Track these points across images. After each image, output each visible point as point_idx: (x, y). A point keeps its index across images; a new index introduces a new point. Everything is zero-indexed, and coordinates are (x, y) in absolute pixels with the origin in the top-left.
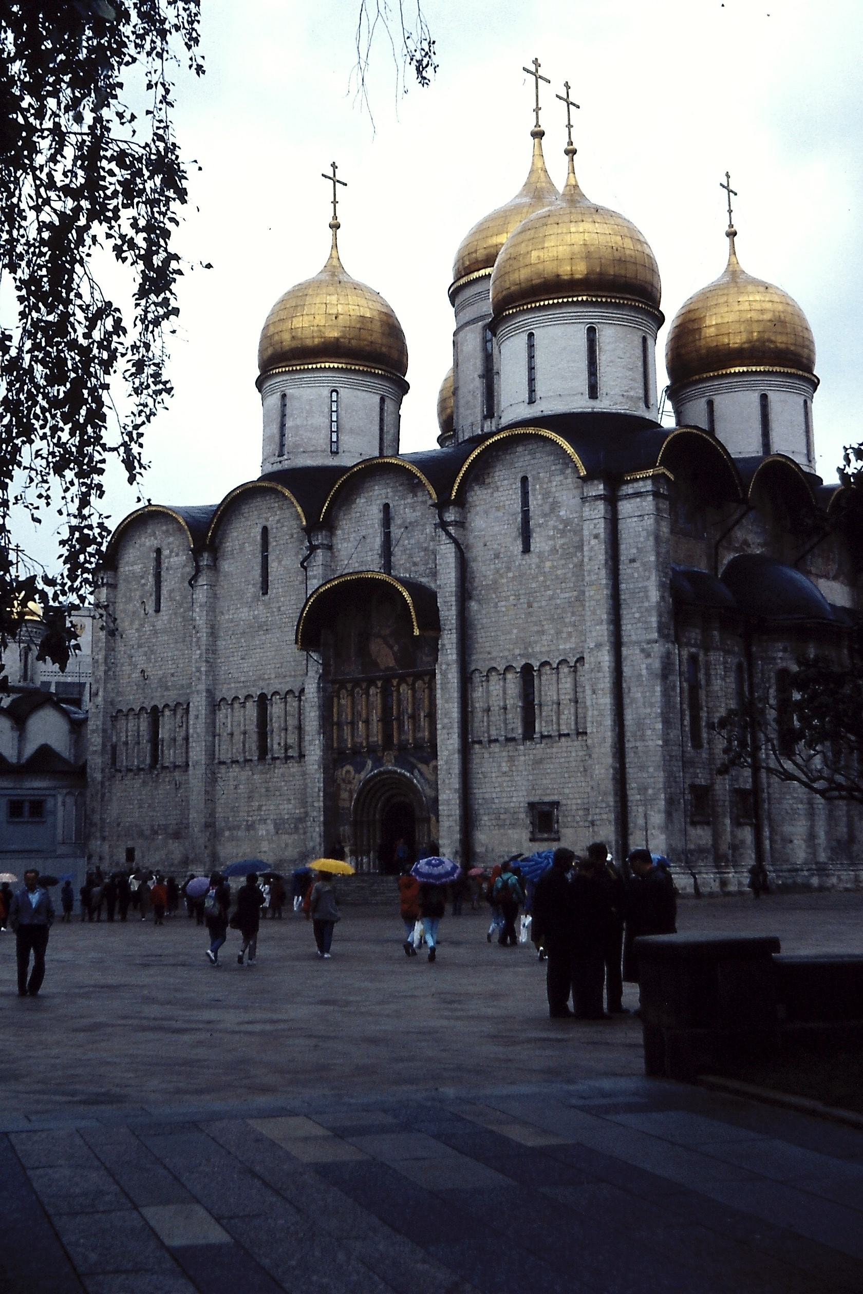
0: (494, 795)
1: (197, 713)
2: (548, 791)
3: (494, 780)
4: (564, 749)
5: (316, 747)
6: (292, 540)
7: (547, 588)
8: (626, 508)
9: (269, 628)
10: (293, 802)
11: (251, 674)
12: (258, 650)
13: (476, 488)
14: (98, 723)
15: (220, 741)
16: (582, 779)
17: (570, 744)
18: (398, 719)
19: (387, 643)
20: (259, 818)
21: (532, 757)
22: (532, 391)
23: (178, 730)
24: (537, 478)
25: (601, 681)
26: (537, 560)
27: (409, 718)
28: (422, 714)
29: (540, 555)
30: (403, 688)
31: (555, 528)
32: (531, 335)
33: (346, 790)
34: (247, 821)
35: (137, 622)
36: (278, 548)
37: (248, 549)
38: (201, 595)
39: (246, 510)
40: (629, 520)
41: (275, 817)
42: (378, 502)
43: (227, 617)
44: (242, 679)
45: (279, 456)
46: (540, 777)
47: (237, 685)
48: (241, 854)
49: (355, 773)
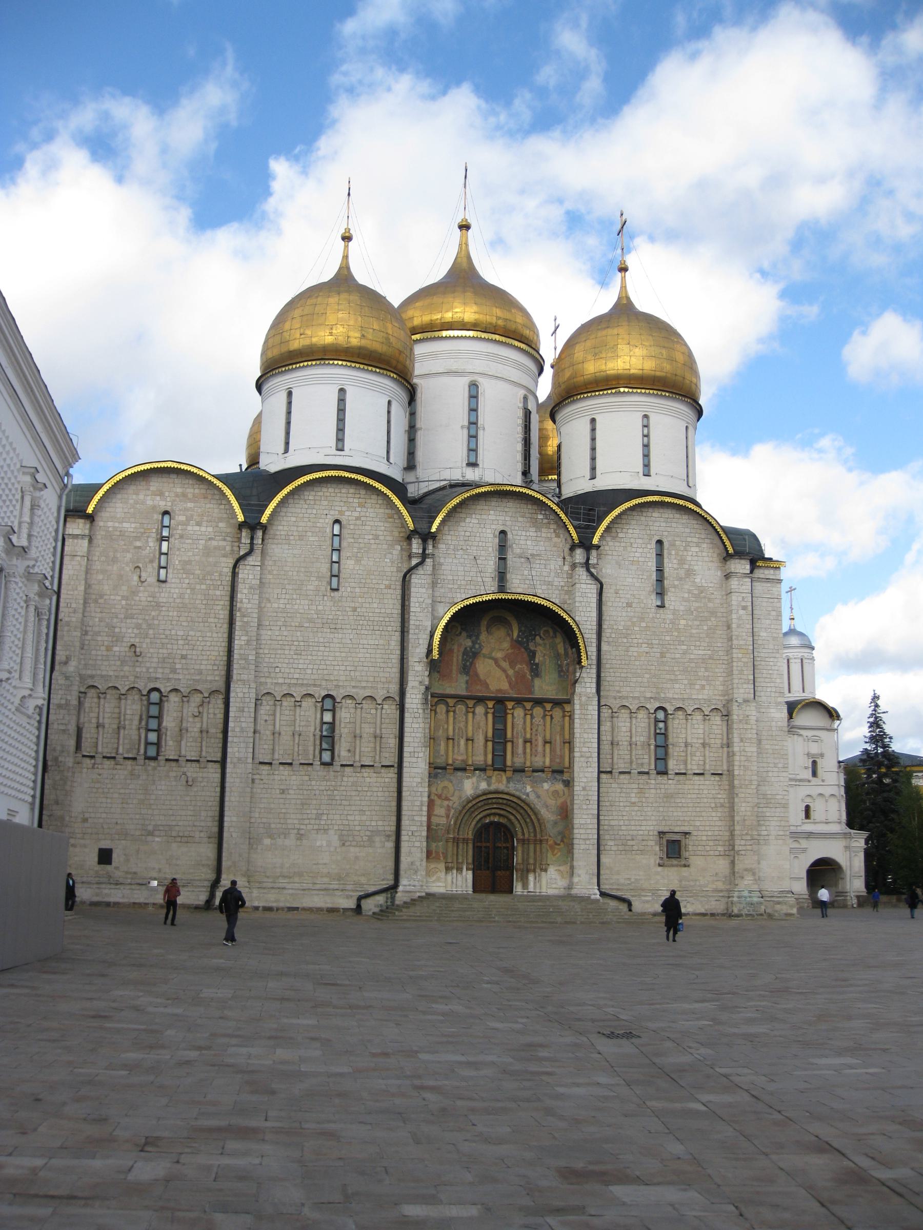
0: (621, 823)
1: (241, 705)
2: (679, 823)
3: (621, 808)
4: (696, 787)
5: (419, 760)
6: (377, 541)
7: (682, 643)
9: (339, 626)
10: (367, 813)
11: (309, 671)
12: (322, 649)
13: (608, 539)
14: (69, 697)
15: (259, 739)
16: (714, 814)
17: (702, 782)
18: (512, 742)
19: (499, 666)
20: (316, 827)
21: (663, 791)
22: (647, 466)
23: (191, 719)
24: (673, 544)
25: (749, 731)
26: (671, 617)
27: (525, 742)
29: (675, 612)
30: (519, 712)
31: (689, 592)
32: (646, 416)
34: (299, 829)
35: (124, 588)
36: (356, 545)
37: (311, 539)
38: (248, 574)
40: (760, 599)
41: (341, 827)
42: (493, 527)
43: (276, 605)
44: (296, 676)
45: (338, 450)
46: (671, 809)
47: (287, 681)
48: (287, 865)
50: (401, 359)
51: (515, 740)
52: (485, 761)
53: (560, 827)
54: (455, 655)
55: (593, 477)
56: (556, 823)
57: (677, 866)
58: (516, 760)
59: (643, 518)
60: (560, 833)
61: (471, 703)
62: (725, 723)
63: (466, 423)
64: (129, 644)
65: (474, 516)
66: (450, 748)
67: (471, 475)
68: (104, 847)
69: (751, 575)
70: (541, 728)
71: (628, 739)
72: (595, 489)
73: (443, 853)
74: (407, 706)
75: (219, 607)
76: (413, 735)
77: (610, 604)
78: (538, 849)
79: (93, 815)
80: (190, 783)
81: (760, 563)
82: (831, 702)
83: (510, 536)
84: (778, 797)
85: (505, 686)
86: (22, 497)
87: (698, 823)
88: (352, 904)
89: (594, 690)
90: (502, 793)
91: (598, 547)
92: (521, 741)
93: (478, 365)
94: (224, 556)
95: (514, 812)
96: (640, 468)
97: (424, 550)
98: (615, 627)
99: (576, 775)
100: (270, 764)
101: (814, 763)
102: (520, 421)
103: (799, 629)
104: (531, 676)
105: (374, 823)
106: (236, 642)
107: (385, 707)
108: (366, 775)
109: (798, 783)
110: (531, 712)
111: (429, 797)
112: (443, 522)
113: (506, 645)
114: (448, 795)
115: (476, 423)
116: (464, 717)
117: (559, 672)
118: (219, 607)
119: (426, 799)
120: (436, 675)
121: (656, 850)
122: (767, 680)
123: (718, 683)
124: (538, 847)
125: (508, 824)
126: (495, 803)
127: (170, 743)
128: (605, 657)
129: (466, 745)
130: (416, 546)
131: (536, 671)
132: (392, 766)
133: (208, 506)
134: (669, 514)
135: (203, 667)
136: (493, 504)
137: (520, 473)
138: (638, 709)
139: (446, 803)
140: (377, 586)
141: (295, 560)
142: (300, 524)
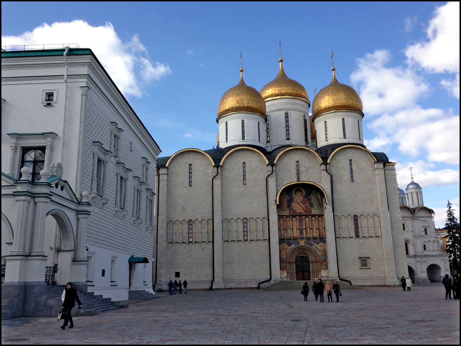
8: (387, 172)
14: (164, 225)
19: (299, 205)
20: (244, 261)
22: (345, 135)
27: (310, 230)
28: (315, 228)
30: (307, 219)
32: (343, 119)
33: (284, 252)
38: (217, 182)
39: (235, 156)
44: (234, 213)
45: (243, 139)
47: (232, 214)
49: (288, 246)
50: (261, 108)
51: (306, 229)
52: (297, 236)
53: (323, 257)
54: (285, 202)
55: (327, 141)
56: (322, 255)
57: (366, 269)
58: (307, 235)
59: (344, 153)
61: (291, 218)
62: (378, 219)
63: (285, 126)
64: (182, 206)
65: (288, 157)
66: (285, 232)
67: (288, 143)
68: (177, 272)
69: (384, 168)
70: (314, 224)
72: (328, 144)
74: (270, 220)
75: (209, 193)
76: (273, 229)
77: (335, 182)
78: (317, 265)
79: (173, 261)
80: (203, 249)
81: (387, 164)
82: (430, 208)
83: (300, 162)
84: (401, 244)
85: (302, 211)
86: (143, 167)
87: (372, 254)
88: (257, 286)
89: (332, 211)
90: (303, 246)
91: (329, 163)
92: (308, 229)
93: (288, 106)
94: (210, 176)
96: (343, 137)
97: (272, 169)
100: (228, 241)
101: (426, 230)
102: (303, 123)
103: (415, 182)
105: (262, 259)
106: (215, 203)
107: (263, 220)
108: (259, 243)
109: (420, 237)
110: (311, 219)
111: (279, 249)
112: (278, 160)
113: (301, 198)
114: (286, 248)
115: (288, 126)
118: (209, 193)
119: (278, 250)
120: (278, 209)
121: (358, 263)
122: (393, 204)
123: (375, 206)
124: (317, 264)
125: (307, 257)
126: (302, 250)
127: (196, 237)
128: (335, 199)
129: (290, 231)
130: (270, 168)
131: (312, 205)
132: (267, 240)
133: (203, 161)
134: (353, 150)
135: (205, 212)
136: (294, 152)
137: (304, 141)
138: (347, 216)
139: (285, 250)
140: (258, 182)
141: (232, 176)
142: (232, 164)
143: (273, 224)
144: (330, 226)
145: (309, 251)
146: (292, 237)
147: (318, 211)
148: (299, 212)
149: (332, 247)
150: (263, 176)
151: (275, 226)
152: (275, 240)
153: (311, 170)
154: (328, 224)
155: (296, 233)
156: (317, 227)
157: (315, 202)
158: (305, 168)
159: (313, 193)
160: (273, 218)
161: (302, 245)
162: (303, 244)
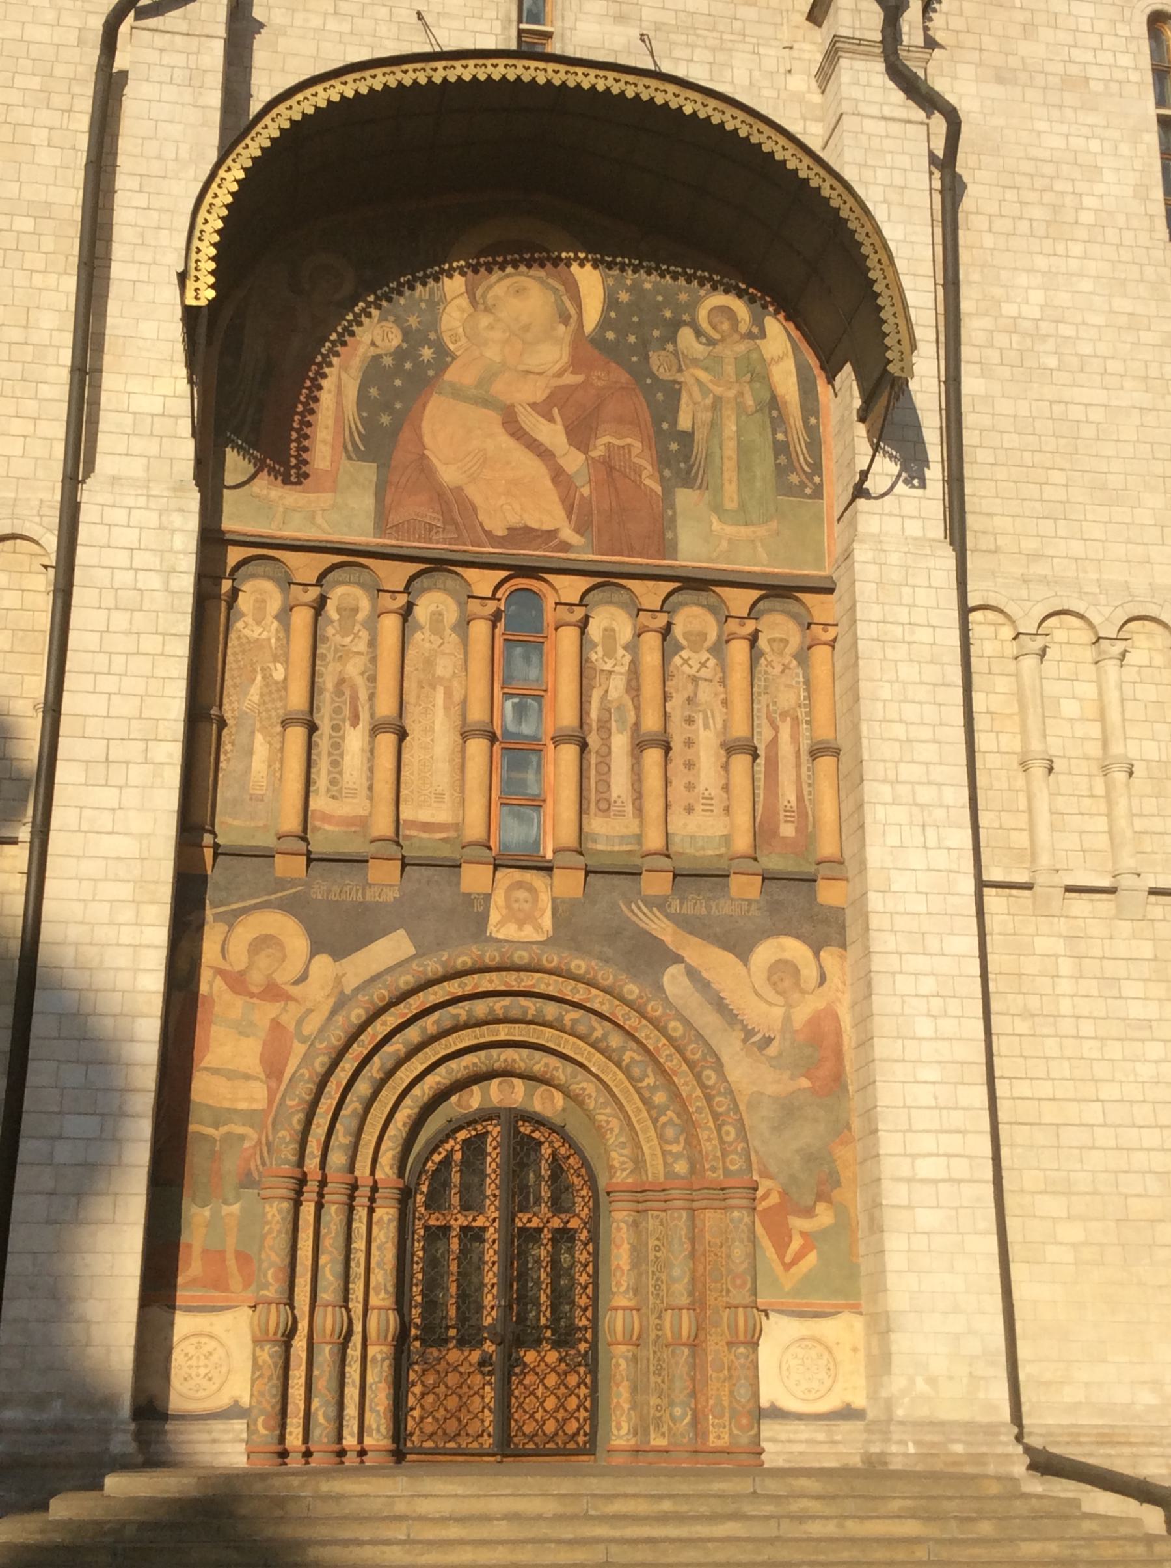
0: (1093, 1113)
3: (1090, 1049)
27: (639, 745)
33: (243, 1029)
51: (593, 740)
52: (458, 827)
53: (807, 1135)
58: (597, 825)
60: (810, 1158)
61: (395, 575)
70: (705, 693)
71: (1094, 749)
73: (243, 1258)
76: (108, 684)
89: (937, 530)
92: (620, 743)
95: (596, 1062)
98: (1010, 309)
99: (874, 879)
104: (662, 480)
116: (365, 634)
117: (781, 471)
143: (120, 620)
144: (910, 712)
145: (615, 1040)
146: (383, 826)
147: (762, 531)
148: (514, 520)
149: (928, 985)
150: (73, 38)
151: (150, 644)
152: (124, 846)
153: (699, 54)
154: (885, 692)
155: (442, 775)
156: (740, 730)
157: (731, 428)
158: (620, 18)
159: (704, 324)
160: (128, 537)
161: (521, 956)
162: (529, 934)
